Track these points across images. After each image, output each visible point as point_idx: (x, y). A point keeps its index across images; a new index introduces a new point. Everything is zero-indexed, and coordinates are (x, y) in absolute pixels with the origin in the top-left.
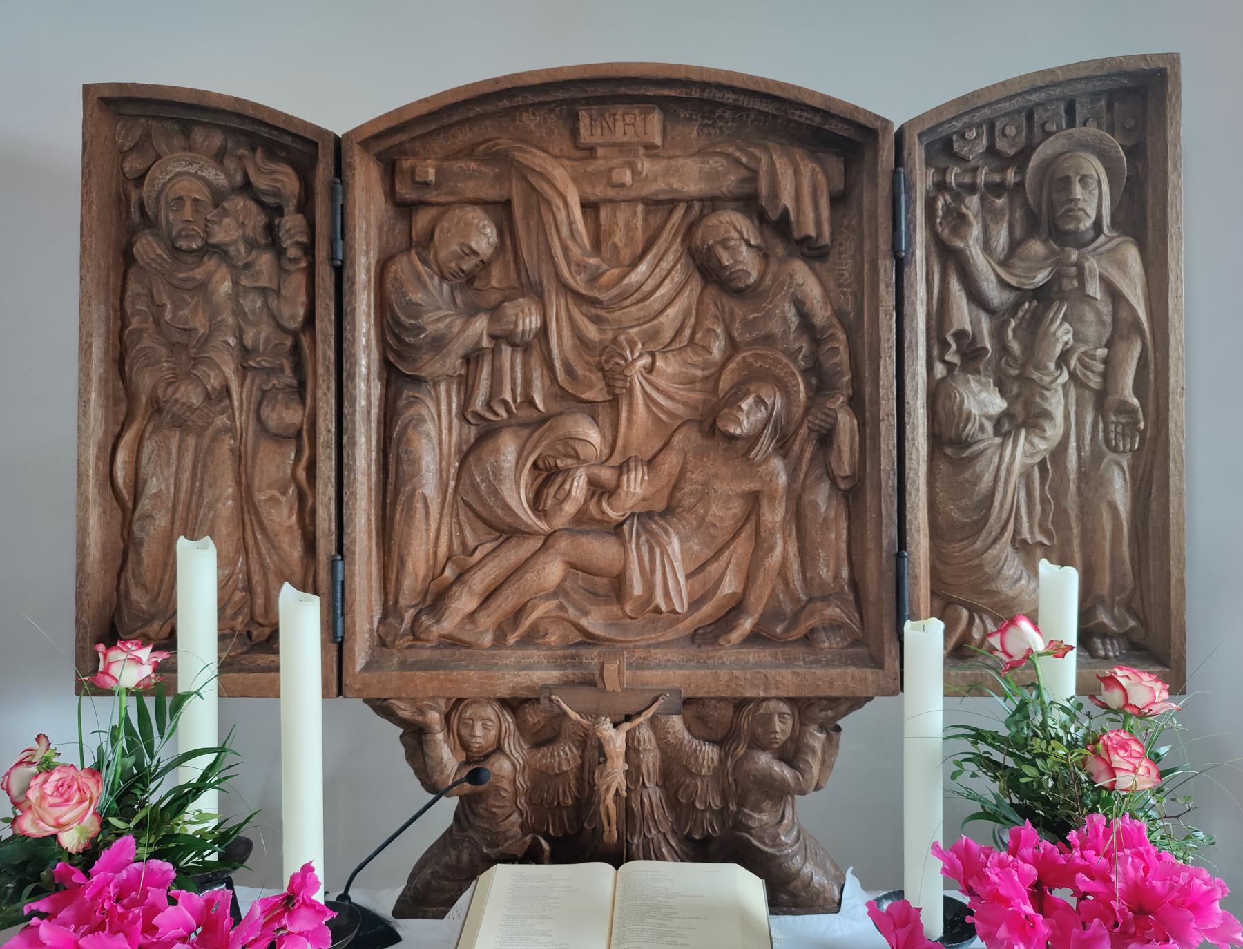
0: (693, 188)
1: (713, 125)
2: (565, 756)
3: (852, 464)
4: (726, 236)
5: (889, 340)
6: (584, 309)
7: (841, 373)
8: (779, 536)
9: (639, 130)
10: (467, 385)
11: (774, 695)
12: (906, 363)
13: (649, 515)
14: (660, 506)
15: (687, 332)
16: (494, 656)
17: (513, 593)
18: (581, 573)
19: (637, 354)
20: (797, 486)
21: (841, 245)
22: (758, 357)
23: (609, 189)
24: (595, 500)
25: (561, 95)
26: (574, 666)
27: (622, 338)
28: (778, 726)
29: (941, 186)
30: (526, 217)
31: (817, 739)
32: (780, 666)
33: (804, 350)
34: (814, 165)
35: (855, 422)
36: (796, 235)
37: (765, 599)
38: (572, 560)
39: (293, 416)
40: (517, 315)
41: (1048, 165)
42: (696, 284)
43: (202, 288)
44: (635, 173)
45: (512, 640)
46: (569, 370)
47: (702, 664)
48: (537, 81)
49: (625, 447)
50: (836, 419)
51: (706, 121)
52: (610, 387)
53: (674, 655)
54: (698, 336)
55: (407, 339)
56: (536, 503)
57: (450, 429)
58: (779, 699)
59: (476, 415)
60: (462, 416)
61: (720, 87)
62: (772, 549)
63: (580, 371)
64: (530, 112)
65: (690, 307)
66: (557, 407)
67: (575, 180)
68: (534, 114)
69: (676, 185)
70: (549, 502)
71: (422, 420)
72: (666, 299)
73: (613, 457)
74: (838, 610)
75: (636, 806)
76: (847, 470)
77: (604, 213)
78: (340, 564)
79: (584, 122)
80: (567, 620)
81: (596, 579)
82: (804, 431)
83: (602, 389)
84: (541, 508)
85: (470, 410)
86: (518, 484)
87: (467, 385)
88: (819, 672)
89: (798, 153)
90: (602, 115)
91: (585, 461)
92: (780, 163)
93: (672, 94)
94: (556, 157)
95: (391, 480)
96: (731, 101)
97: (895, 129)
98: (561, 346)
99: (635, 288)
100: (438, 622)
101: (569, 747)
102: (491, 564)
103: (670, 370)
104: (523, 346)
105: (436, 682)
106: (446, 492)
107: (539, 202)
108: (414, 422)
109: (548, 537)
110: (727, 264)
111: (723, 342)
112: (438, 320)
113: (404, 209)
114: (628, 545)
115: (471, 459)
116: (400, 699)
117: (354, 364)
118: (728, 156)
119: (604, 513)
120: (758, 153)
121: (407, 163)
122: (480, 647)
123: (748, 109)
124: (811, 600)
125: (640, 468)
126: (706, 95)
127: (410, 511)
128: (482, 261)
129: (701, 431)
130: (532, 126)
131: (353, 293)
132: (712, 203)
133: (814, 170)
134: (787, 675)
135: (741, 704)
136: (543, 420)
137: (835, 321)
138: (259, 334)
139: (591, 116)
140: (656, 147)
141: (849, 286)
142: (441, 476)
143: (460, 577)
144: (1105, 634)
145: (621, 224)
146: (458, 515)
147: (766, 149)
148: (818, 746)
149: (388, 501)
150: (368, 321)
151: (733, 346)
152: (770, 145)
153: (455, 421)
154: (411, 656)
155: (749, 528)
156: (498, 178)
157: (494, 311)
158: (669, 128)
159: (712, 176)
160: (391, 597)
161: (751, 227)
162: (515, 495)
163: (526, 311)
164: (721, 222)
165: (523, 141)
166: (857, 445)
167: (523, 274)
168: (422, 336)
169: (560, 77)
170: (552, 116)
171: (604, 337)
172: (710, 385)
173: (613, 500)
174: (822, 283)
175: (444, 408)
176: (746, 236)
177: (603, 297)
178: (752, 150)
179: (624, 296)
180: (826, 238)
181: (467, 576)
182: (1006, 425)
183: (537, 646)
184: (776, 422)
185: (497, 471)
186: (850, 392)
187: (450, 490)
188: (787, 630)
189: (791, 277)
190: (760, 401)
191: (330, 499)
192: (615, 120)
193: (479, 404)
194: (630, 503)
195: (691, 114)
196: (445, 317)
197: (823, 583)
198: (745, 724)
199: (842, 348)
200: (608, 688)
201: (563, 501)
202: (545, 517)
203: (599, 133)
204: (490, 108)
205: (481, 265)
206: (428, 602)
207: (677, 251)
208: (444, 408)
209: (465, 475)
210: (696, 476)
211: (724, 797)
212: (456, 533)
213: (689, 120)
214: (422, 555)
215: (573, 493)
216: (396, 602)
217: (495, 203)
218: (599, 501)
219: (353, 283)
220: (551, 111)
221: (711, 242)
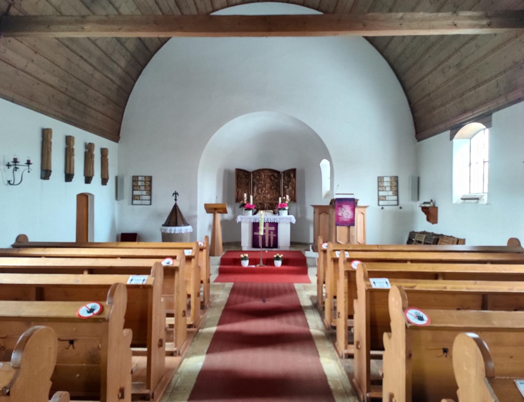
2: (262, 206)
39: (247, 187)
87: (257, 186)
107: (261, 176)
113: (253, 175)
132: (271, 176)
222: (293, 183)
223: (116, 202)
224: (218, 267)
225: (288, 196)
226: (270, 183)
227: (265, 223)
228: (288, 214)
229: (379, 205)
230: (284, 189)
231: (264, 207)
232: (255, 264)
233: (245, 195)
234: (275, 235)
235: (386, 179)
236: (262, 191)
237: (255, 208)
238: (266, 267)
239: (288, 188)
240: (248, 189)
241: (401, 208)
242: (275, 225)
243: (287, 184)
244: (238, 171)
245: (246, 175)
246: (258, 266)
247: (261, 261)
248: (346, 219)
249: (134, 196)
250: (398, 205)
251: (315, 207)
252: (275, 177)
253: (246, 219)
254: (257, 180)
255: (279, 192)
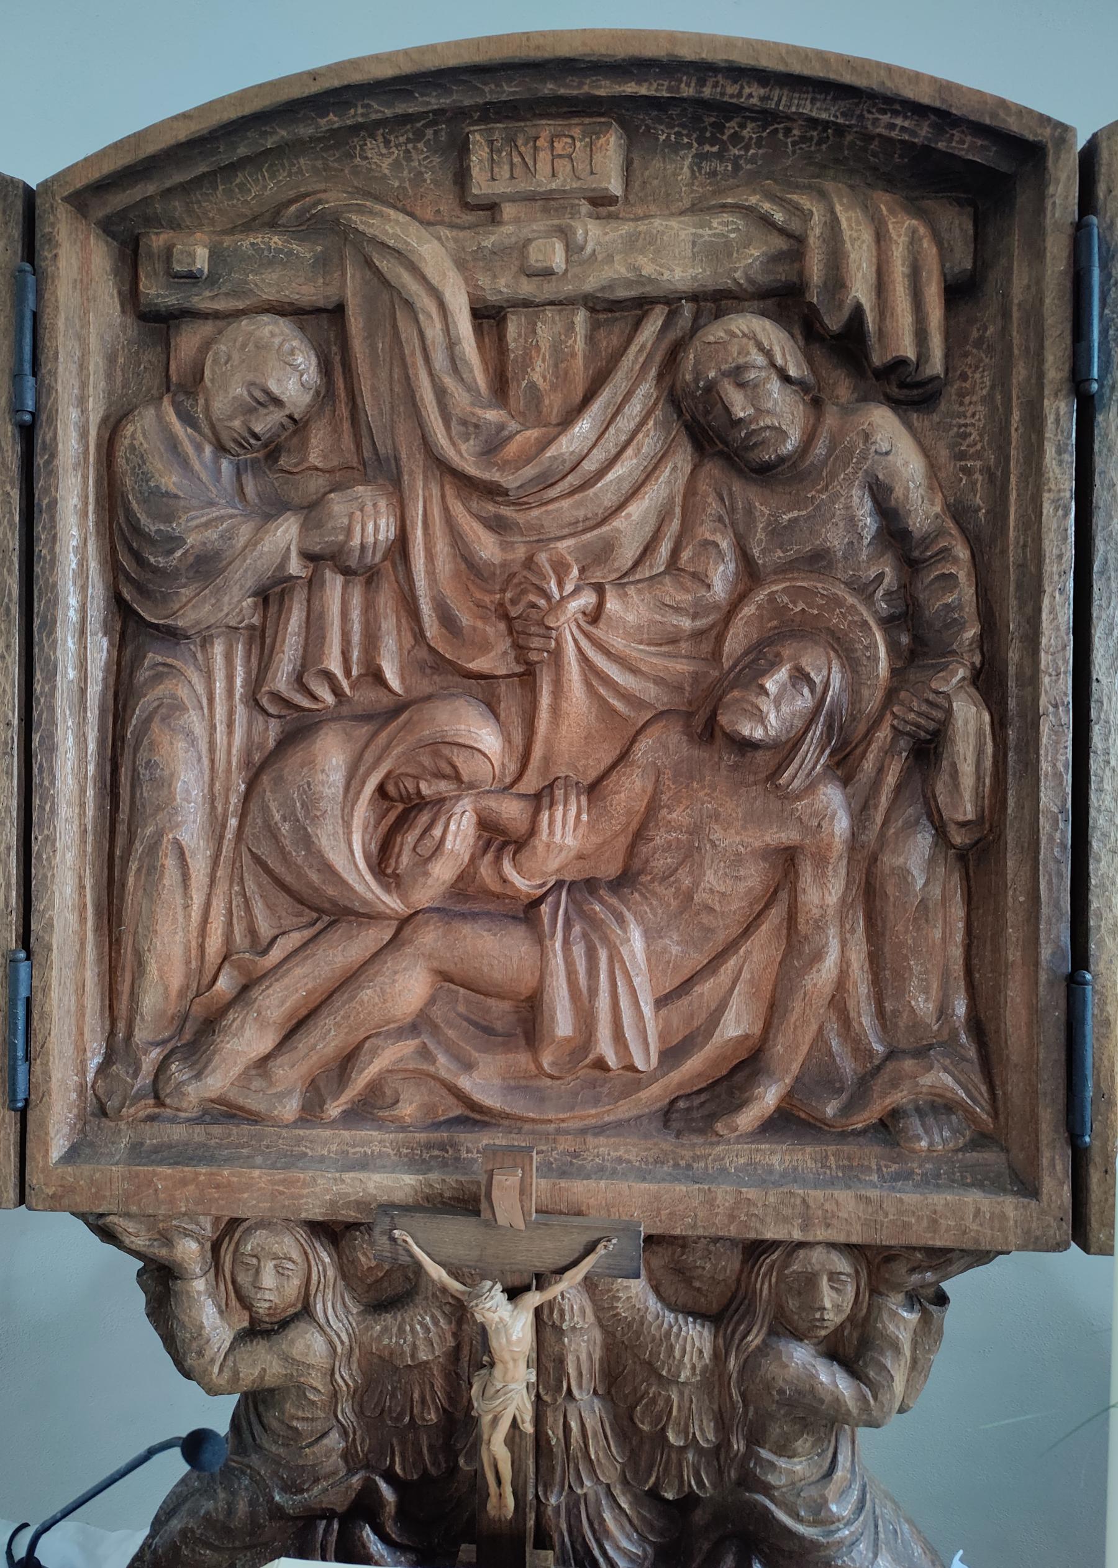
1: (720, 156)
3: (978, 795)
4: (741, 361)
5: (1060, 556)
6: (474, 505)
7: (961, 626)
8: (832, 932)
9: (582, 167)
11: (820, 1238)
12: (1096, 603)
13: (590, 885)
14: (611, 869)
15: (664, 549)
16: (299, 1140)
17: (338, 1025)
18: (462, 990)
19: (569, 588)
20: (870, 836)
21: (964, 377)
22: (796, 593)
23: (524, 280)
24: (489, 857)
25: (435, 101)
26: (444, 1164)
27: (542, 558)
28: (828, 1297)
30: (370, 336)
32: (832, 1182)
33: (886, 580)
34: (914, 222)
35: (987, 717)
36: (877, 359)
37: (805, 1049)
38: (445, 968)
40: (351, 515)
42: (682, 459)
44: (572, 249)
45: (334, 1110)
46: (447, 619)
47: (686, 1173)
48: (388, 72)
49: (547, 760)
50: (949, 711)
51: (707, 148)
52: (520, 649)
53: (631, 1150)
54: (686, 555)
55: (152, 560)
57: (230, 725)
58: (832, 1245)
59: (276, 697)
60: (253, 701)
61: (737, 72)
62: (818, 956)
63: (465, 619)
64: (380, 139)
65: (671, 499)
66: (424, 686)
67: (461, 265)
68: (387, 143)
69: (649, 269)
70: (405, 860)
71: (180, 707)
72: (626, 486)
73: (525, 778)
74: (949, 1080)
75: (555, 1435)
76: (968, 810)
77: (513, 328)
78: (23, 967)
79: (479, 155)
80: (435, 1078)
81: (491, 1002)
82: (883, 734)
83: (505, 653)
84: (389, 871)
85: (265, 689)
86: (347, 825)
88: (911, 1198)
89: (883, 201)
90: (511, 141)
91: (471, 786)
92: (849, 219)
93: (643, 91)
94: (426, 223)
95: (123, 815)
96: (754, 101)
97: (1081, 143)
98: (431, 574)
99: (568, 466)
100: (198, 1076)
101: (433, 1317)
102: (298, 971)
103: (631, 618)
105: (192, 1187)
106: (222, 837)
108: (164, 710)
109: (404, 922)
110: (742, 415)
111: (732, 566)
112: (207, 525)
114: (548, 942)
115: (265, 778)
116: (127, 1215)
117: (53, 603)
118: (748, 211)
119: (505, 881)
120: (805, 201)
121: (157, 240)
122: (276, 1123)
123: (788, 118)
124: (892, 1054)
125: (573, 799)
126: (707, 92)
127: (152, 870)
128: (290, 417)
129: (688, 731)
130: (385, 165)
131: (52, 473)
133: (914, 231)
136: (399, 708)
137: (950, 524)
139: (491, 143)
140: (612, 200)
141: (978, 456)
142: (213, 808)
143: (245, 990)
145: (545, 346)
146: (242, 879)
147: (822, 195)
148: (905, 1338)
149: (118, 853)
150: (82, 526)
152: (829, 186)
153: (240, 711)
154: (153, 1135)
155: (776, 915)
156: (323, 264)
158: (636, 164)
159: (719, 251)
160: (121, 1025)
161: (789, 344)
162: (343, 846)
163: (369, 508)
164: (733, 335)
165: (367, 194)
166: (988, 763)
167: (366, 442)
168: (178, 553)
169: (431, 63)
170: (420, 145)
171: (510, 556)
172: (706, 647)
173: (522, 857)
174: (926, 452)
175: (219, 686)
176: (779, 361)
177: (509, 481)
178: (795, 197)
179: (545, 480)
180: (936, 365)
181: (255, 993)
183: (380, 1124)
184: (831, 715)
185: (310, 802)
186: (977, 660)
187: (229, 835)
188: (847, 1110)
189: (867, 437)
190: (800, 676)
191: (9, 848)
192: (535, 148)
193: (281, 680)
194: (554, 864)
195: (678, 134)
196: (221, 519)
197: (916, 1024)
198: (764, 1290)
199: (962, 576)
200: (502, 1220)
201: (429, 859)
202: (398, 886)
203: (508, 175)
204: (305, 131)
205: (291, 427)
206: (187, 1036)
207: (647, 396)
208: (219, 686)
209: (254, 807)
210: (678, 815)
211: (723, 1425)
212: (238, 912)
213: (676, 147)
214: (178, 951)
215: (448, 845)
216: (129, 1035)
217: (317, 311)
218: (498, 859)
219: (53, 455)
220: (419, 135)
221: (712, 374)
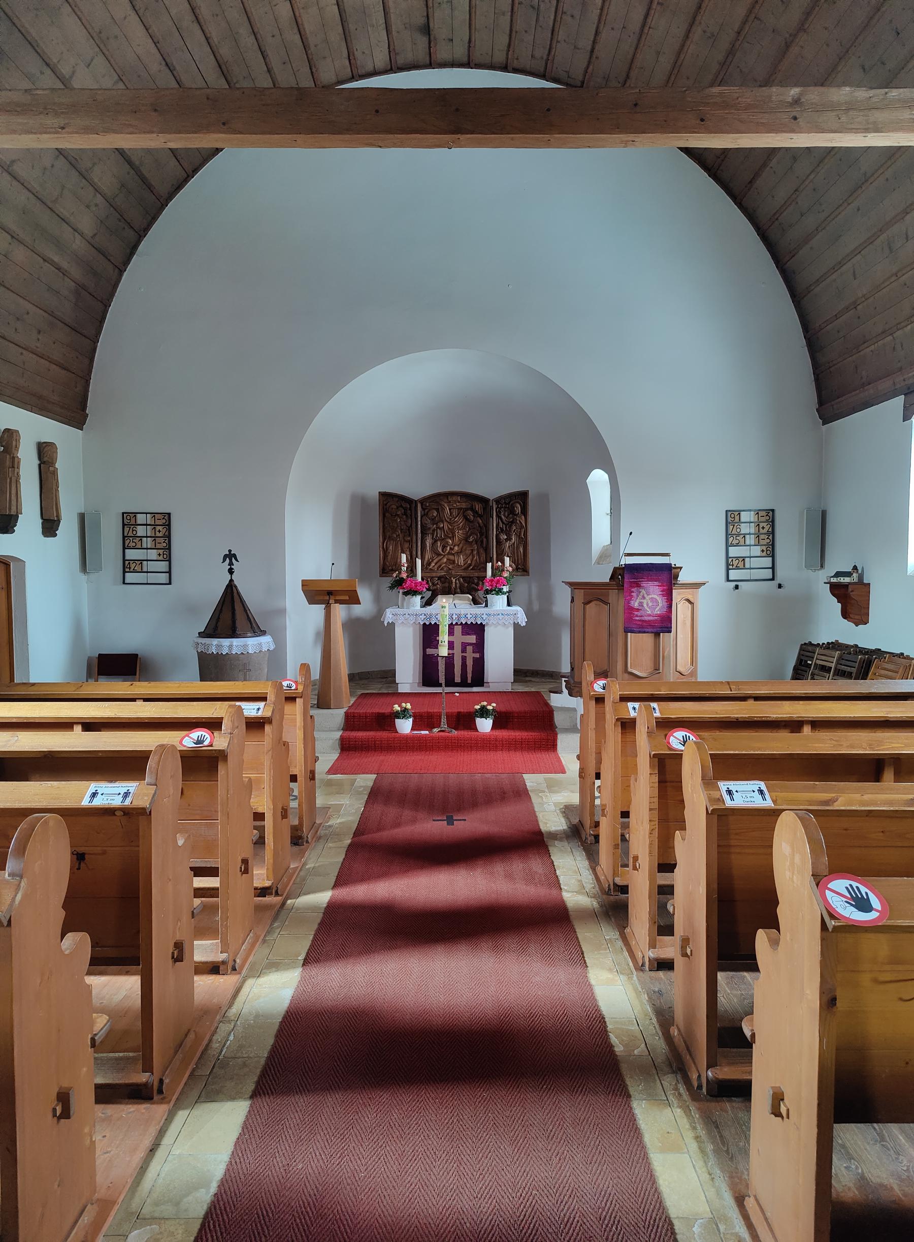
0: (464, 507)
2: (447, 585)
10: (433, 535)
29: (498, 507)
31: (481, 583)
39: (409, 538)
41: (512, 505)
43: (396, 520)
56: (442, 551)
87: (433, 535)
104: (440, 529)
107: (443, 509)
109: (444, 556)
113: (423, 509)
132: (467, 509)
134: (476, 574)
135: (470, 577)
136: (443, 539)
138: (404, 527)
144: (519, 568)
151: (470, 529)
157: (437, 524)
182: (506, 540)
222: (522, 527)
223: (83, 577)
224: (338, 734)
225: (507, 560)
226: (463, 528)
227: (451, 627)
228: (509, 604)
229: (728, 580)
230: (499, 542)
231: (450, 587)
232: (430, 727)
233: (404, 558)
234: (477, 655)
235: (745, 517)
236: (444, 547)
237: (428, 590)
238: (455, 733)
239: (509, 539)
240: (410, 542)
241: (780, 586)
242: (478, 629)
243: (505, 529)
244: (387, 498)
245: (405, 509)
246: (436, 730)
247: (444, 720)
248: (649, 615)
249: (127, 562)
250: (773, 579)
251: (574, 586)
252: (475, 512)
253: (407, 616)
254: (433, 519)
255: (487, 549)
